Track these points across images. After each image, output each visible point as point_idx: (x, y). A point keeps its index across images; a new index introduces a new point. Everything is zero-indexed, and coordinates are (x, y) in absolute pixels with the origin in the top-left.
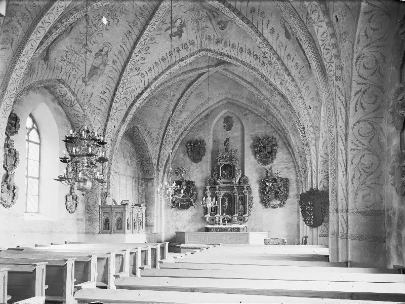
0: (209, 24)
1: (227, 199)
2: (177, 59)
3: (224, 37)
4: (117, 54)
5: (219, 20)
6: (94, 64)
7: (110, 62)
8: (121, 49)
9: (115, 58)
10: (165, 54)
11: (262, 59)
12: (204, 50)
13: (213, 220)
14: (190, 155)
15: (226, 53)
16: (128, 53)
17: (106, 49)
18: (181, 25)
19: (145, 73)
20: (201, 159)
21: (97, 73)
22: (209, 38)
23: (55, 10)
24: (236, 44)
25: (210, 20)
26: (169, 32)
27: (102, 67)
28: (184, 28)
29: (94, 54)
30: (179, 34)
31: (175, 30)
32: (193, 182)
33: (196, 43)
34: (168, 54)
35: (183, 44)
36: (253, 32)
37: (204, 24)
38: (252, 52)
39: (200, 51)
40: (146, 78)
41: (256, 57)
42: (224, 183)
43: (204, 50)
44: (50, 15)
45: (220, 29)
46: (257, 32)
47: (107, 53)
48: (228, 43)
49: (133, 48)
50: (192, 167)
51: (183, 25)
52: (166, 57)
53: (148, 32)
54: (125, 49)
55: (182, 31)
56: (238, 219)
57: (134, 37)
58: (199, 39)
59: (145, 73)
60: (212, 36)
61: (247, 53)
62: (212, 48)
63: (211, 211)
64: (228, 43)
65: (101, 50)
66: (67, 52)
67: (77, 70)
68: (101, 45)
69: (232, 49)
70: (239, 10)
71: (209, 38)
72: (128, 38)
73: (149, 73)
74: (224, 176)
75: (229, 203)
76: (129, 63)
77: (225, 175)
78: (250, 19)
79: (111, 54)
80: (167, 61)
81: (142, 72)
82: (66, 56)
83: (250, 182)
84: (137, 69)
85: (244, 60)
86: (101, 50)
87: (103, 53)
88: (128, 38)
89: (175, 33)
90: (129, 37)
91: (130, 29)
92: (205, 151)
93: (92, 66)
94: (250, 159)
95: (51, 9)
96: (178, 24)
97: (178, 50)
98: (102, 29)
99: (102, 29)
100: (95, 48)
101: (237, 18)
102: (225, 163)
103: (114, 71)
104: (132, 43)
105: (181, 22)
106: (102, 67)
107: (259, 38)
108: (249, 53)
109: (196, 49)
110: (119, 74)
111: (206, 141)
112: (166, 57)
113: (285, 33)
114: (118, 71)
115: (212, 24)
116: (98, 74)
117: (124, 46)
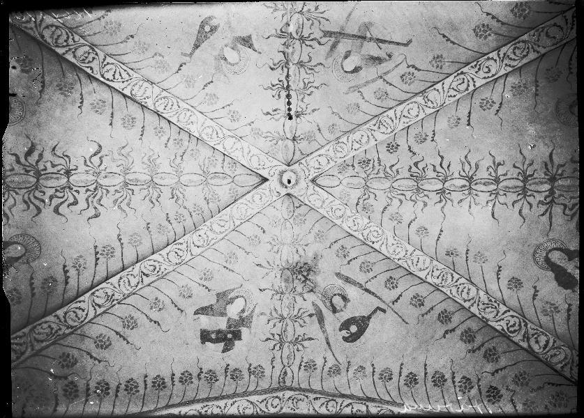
0: (313, 328)
5: (345, 315)
10: (169, 375)
18: (241, 317)
28: (244, 330)
30: (228, 338)
31: (222, 324)
37: (300, 331)
38: (448, 376)
45: (345, 339)
51: (244, 321)
53: (161, 259)
55: (237, 335)
58: (278, 367)
60: (319, 362)
69: (379, 383)
71: (310, 366)
72: (97, 259)
88: (97, 259)
89: (219, 332)
91: (116, 244)
96: (233, 311)
113: (557, 279)
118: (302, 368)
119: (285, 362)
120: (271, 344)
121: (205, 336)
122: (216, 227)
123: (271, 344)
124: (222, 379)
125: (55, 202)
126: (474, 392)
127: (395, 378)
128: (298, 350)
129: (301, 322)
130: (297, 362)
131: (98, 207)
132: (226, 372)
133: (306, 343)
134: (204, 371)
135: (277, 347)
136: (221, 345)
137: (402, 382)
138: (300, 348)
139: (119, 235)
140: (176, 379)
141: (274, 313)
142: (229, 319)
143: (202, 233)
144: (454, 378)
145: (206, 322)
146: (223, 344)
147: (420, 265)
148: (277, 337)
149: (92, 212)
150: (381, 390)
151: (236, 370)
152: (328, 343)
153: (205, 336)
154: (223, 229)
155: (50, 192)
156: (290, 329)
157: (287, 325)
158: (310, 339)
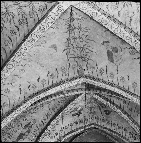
0: (98, 110)
2: (75, 128)
3: (108, 119)
4: (38, 126)
6: (22, 133)
7: (32, 131)
8: (42, 123)
9: (36, 128)
10: (68, 125)
11: (134, 135)
12: (93, 124)
15: (108, 128)
16: (45, 125)
17: (32, 123)
19: (53, 136)
21: (22, 138)
22: (97, 118)
23: (12, 116)
24: (116, 124)
25: (100, 109)
26: (73, 113)
27: (27, 134)
29: (23, 127)
31: (77, 112)
33: (88, 120)
34: (70, 125)
35: (80, 120)
36: (126, 116)
37: (95, 110)
39: (90, 125)
40: (54, 139)
41: (130, 133)
43: (93, 124)
44: (8, 119)
46: (134, 121)
47: (32, 126)
48: (111, 123)
49: (49, 123)
52: (68, 126)
54: (44, 123)
55: (80, 113)
57: (51, 116)
58: (90, 117)
59: (53, 136)
60: (100, 117)
61: (123, 130)
62: (99, 124)
64: (111, 123)
65: (29, 124)
66: (7, 127)
67: (11, 137)
68: (29, 121)
69: (113, 127)
70: (123, 108)
73: (56, 136)
76: (45, 132)
78: (129, 113)
79: (34, 127)
80: (68, 129)
81: (51, 135)
82: (6, 130)
84: (49, 134)
85: (121, 134)
86: (29, 124)
87: (30, 125)
90: (48, 116)
93: (21, 133)
95: (10, 115)
96: (79, 109)
97: (76, 123)
98: (32, 112)
99: (33, 113)
100: (25, 123)
101: (122, 113)
103: (34, 136)
104: (49, 119)
105: (81, 109)
106: (27, 134)
107: (135, 125)
108: (125, 130)
109: (88, 123)
110: (37, 137)
112: (68, 126)
114: (36, 135)
115: (101, 111)
116: (23, 138)
117: (43, 121)
118: (96, 118)
119: (92, 117)
120: (89, 113)
121: (73, 115)
122: (71, 105)
123: (89, 113)
124: (79, 123)
125: (34, 112)
126: (131, 136)
127: (116, 126)
128: (95, 114)
129: (95, 108)
130: (95, 117)
131: (43, 106)
132: (79, 121)
133: (97, 113)
134: (75, 122)
135: (90, 114)
136: (77, 116)
137: (118, 127)
138: (95, 114)
139: (49, 109)
140: (70, 126)
141: (88, 107)
142: (78, 111)
143: (68, 107)
144: (128, 131)
145: (73, 113)
146: (77, 115)
147: (122, 115)
148: (90, 112)
149: (42, 108)
150: (113, 128)
151: (81, 120)
152: (102, 114)
153: (73, 115)
154: (73, 105)
155: (32, 111)
156: (93, 110)
157: (92, 109)
158: (98, 112)
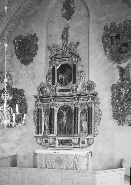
1: (65, 114)
13: (46, 142)
14: (18, 54)
20: (31, 61)
32: (21, 90)
42: (61, 91)
50: (21, 72)
56: (79, 140)
63: (45, 129)
74: (61, 82)
75: (68, 119)
77: (62, 79)
83: (96, 89)
92: (37, 49)
94: (96, 56)
102: (63, 63)
111: (38, 36)
